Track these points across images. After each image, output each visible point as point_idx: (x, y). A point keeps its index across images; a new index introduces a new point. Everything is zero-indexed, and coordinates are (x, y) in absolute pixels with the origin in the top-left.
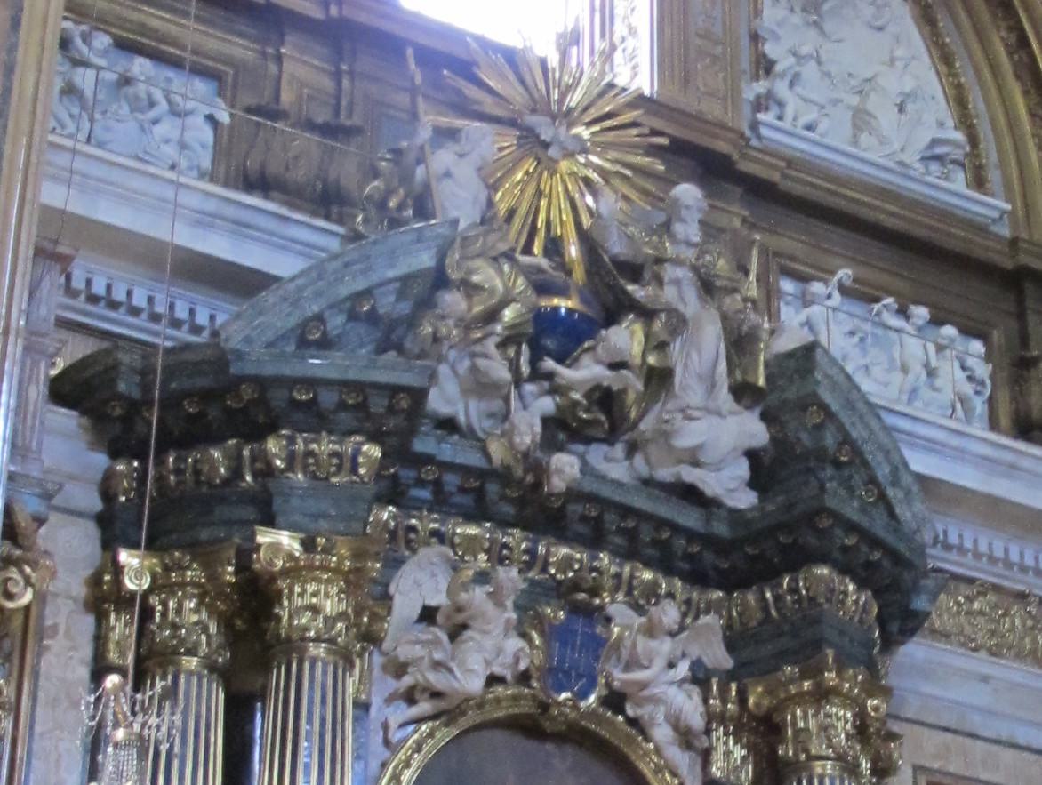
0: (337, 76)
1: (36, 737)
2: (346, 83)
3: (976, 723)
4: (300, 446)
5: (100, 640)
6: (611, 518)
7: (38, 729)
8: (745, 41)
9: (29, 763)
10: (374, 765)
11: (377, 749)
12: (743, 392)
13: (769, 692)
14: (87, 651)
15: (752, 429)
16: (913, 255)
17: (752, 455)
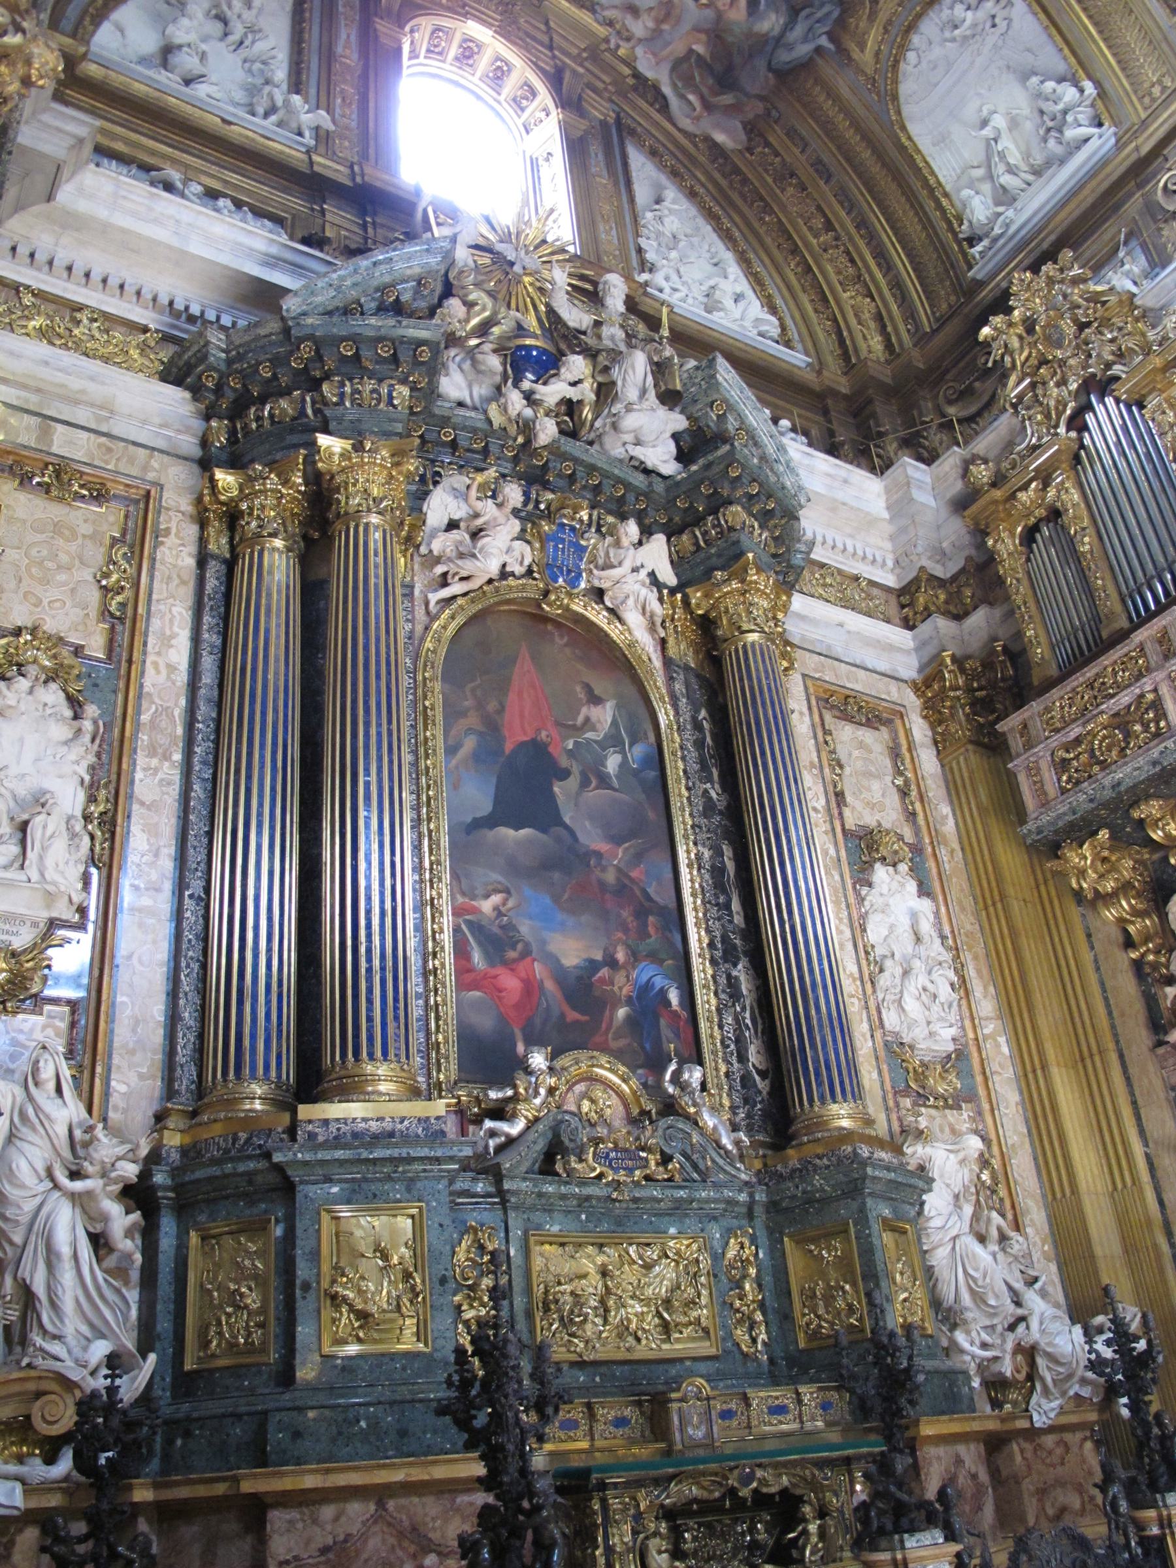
0: (364, 227)
1: (154, 603)
2: (370, 230)
3: (839, 651)
4: (348, 389)
5: (202, 541)
6: (581, 472)
7: (155, 597)
8: (633, 253)
9: (148, 619)
10: (419, 629)
11: (420, 613)
12: (669, 398)
13: (707, 596)
14: (192, 549)
15: (678, 421)
16: (758, 373)
17: (676, 436)
